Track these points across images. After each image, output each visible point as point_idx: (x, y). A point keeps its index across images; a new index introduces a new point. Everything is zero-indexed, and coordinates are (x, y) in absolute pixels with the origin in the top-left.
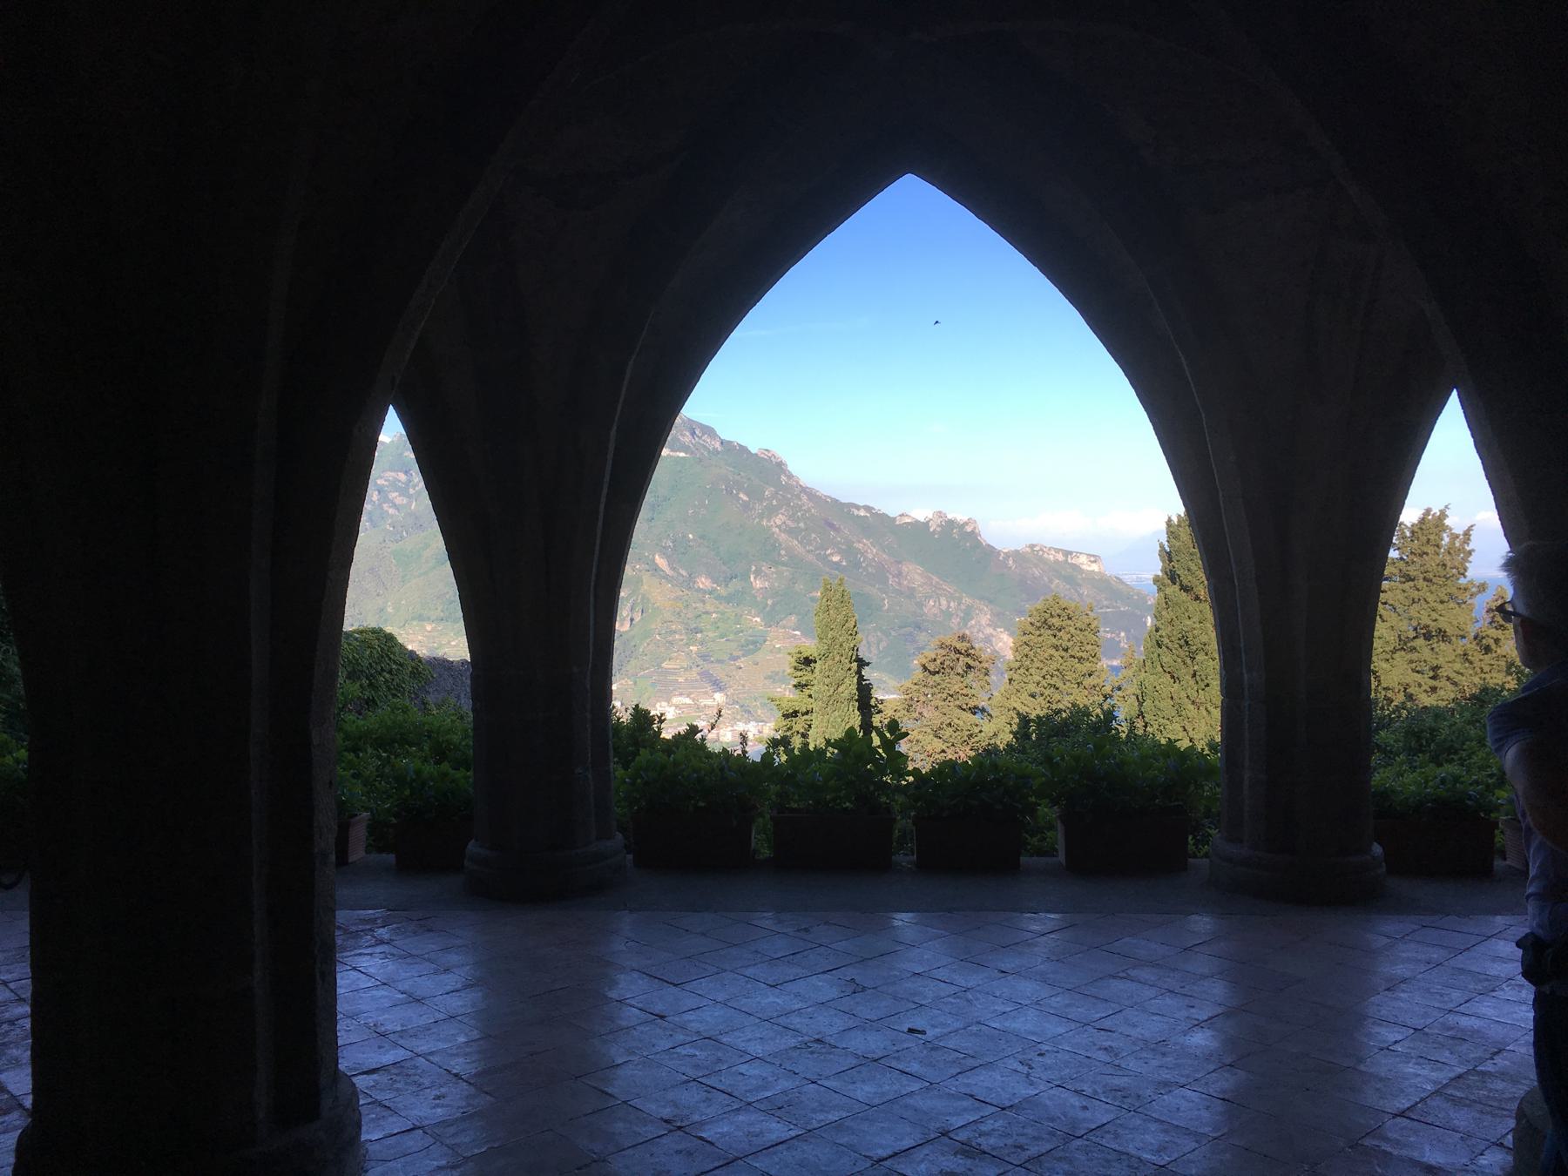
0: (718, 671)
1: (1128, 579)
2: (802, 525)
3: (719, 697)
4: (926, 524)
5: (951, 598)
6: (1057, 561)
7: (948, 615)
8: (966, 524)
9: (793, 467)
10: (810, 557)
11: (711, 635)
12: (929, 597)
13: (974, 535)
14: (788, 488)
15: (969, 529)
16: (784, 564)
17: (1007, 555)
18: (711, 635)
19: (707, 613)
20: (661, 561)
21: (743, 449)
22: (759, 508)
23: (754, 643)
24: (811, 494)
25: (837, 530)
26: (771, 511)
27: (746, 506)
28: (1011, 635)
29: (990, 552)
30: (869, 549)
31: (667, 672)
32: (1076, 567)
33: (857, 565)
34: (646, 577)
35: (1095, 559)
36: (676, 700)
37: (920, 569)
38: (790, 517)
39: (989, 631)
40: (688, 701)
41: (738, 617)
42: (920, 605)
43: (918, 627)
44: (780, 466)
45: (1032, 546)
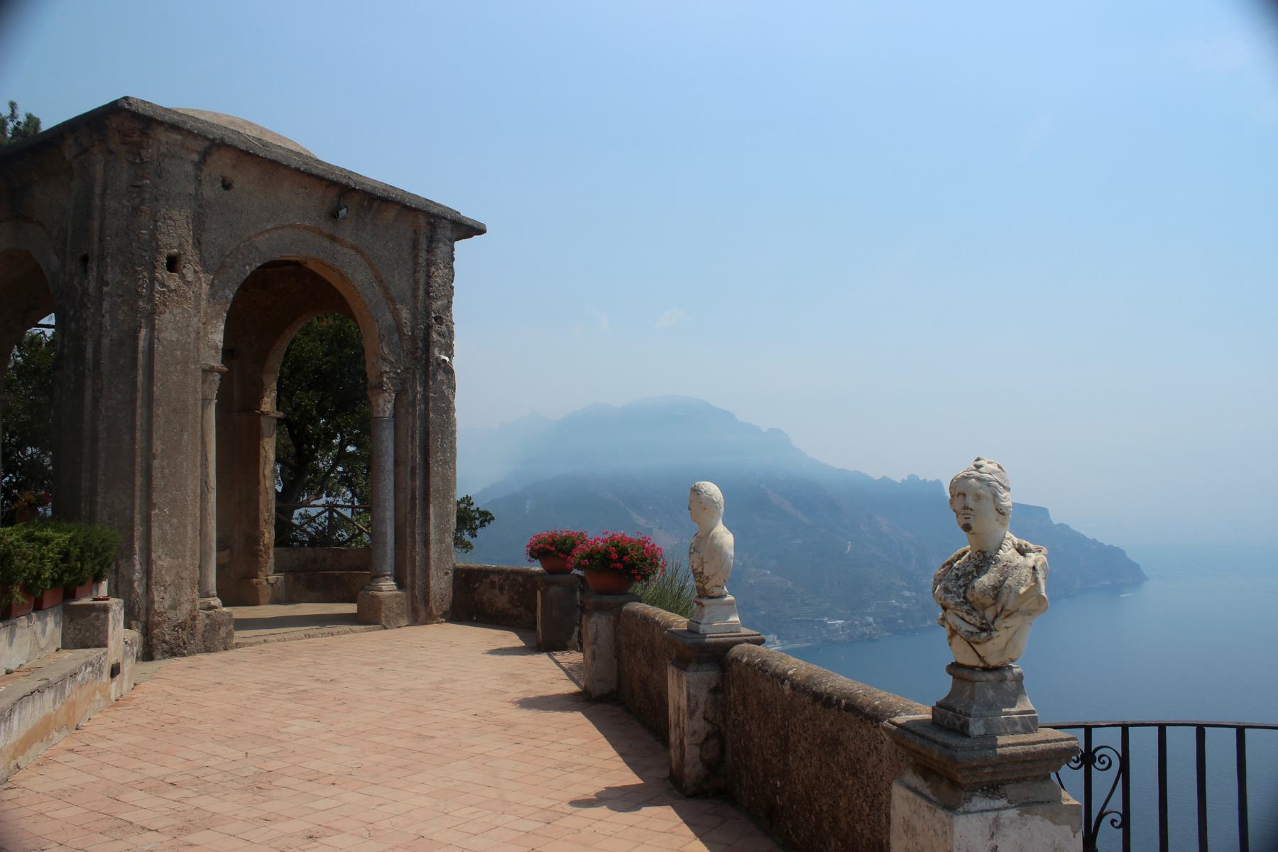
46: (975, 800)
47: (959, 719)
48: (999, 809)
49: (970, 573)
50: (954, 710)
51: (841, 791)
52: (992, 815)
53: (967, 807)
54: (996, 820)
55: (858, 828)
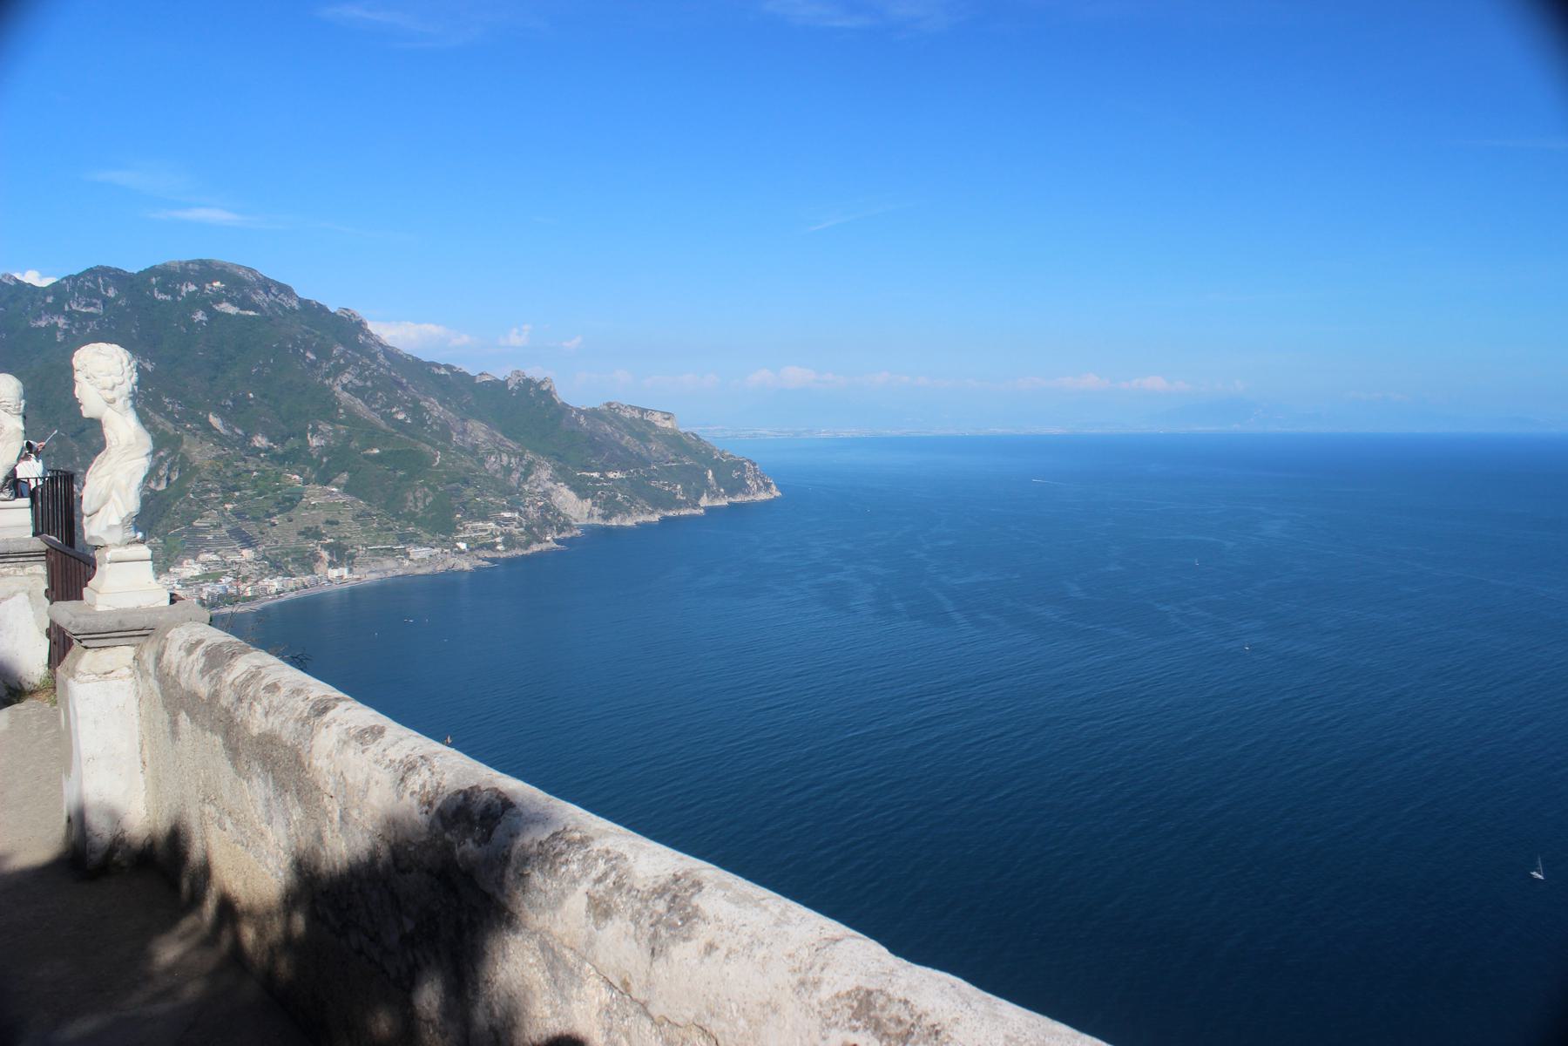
0: (251, 528)
1: (705, 437)
2: (369, 384)
3: (248, 554)
4: (505, 383)
5: (512, 453)
6: (632, 419)
7: (508, 470)
9: (372, 327)
10: (375, 417)
11: (249, 492)
13: (548, 393)
14: (364, 349)
15: (545, 388)
16: (341, 422)
17: (580, 412)
18: (249, 492)
19: (249, 472)
20: (215, 421)
21: (322, 309)
22: (326, 366)
23: (291, 500)
24: (390, 353)
25: (404, 389)
26: (338, 370)
27: (313, 364)
29: (564, 409)
30: (435, 409)
31: (197, 530)
32: (650, 424)
33: (423, 423)
34: (185, 438)
35: (669, 416)
36: (202, 557)
37: (484, 427)
38: (358, 376)
39: (550, 485)
40: (215, 557)
41: (278, 475)
42: (482, 461)
43: (466, 482)
44: (360, 326)
45: (609, 404)
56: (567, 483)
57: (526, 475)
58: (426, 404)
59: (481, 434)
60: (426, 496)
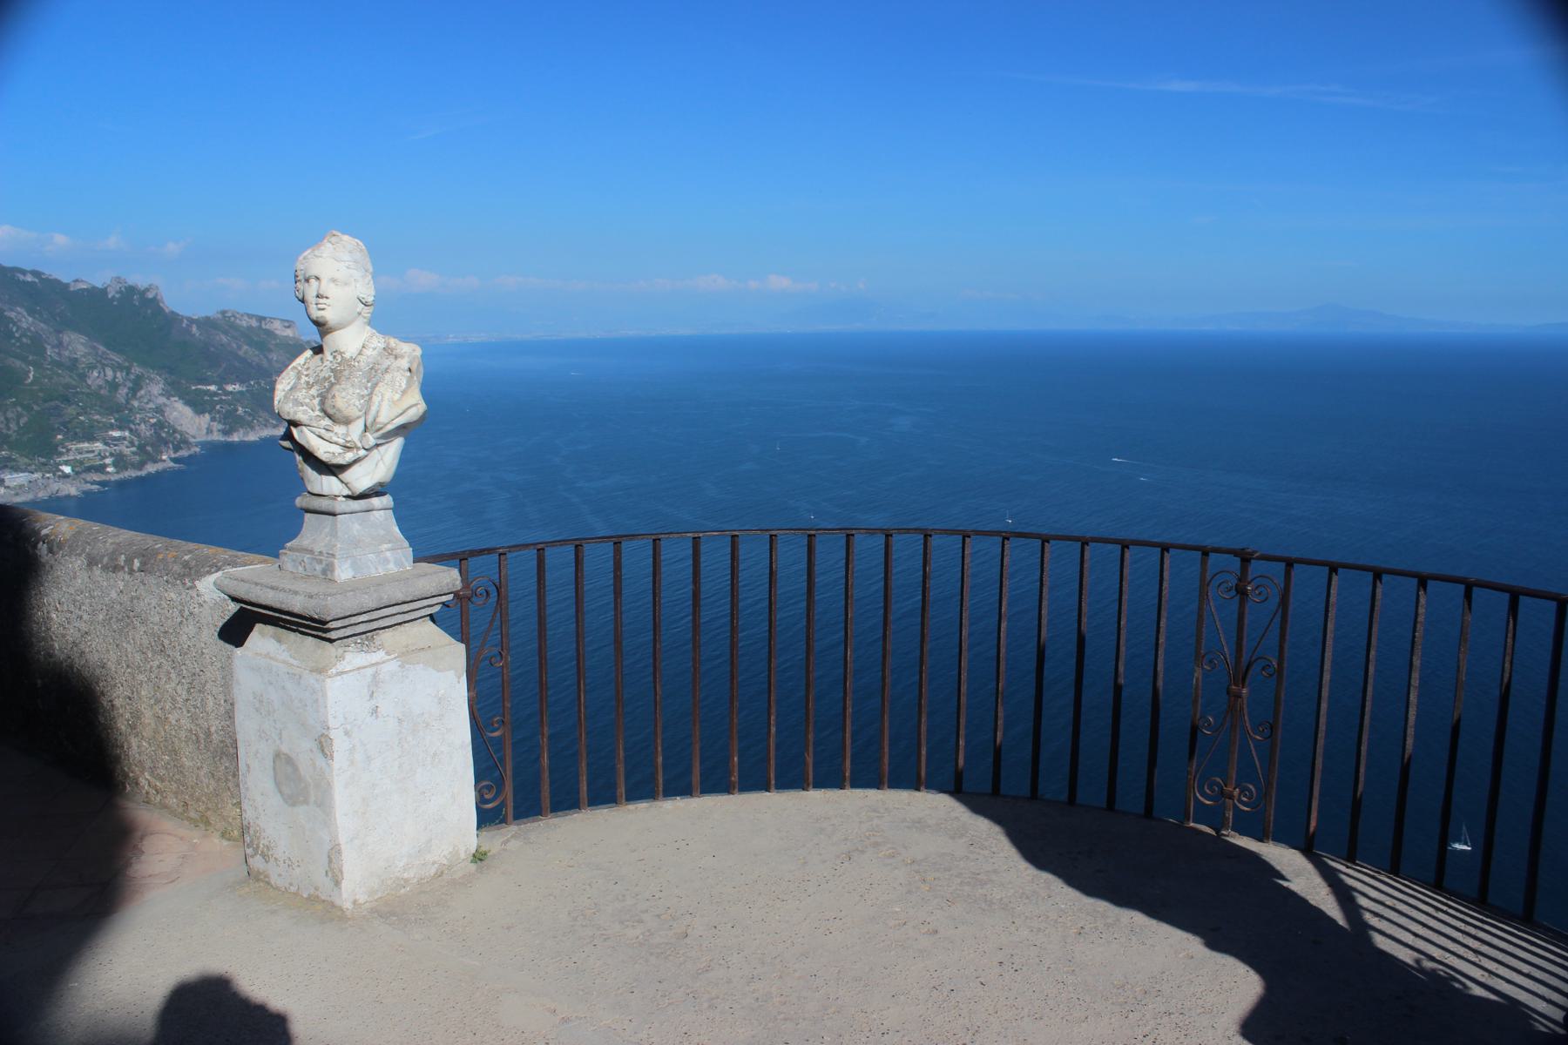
4: (104, 291)
5: (117, 367)
6: (250, 328)
7: (114, 386)
8: (147, 290)
12: (92, 367)
13: (155, 302)
15: (150, 295)
17: (191, 321)
28: (188, 403)
29: (174, 318)
30: (24, 320)
32: (270, 333)
37: (83, 339)
39: (162, 400)
42: (83, 377)
43: (66, 400)
45: (224, 312)
46: (348, 656)
47: (320, 562)
48: (377, 664)
49: (325, 379)
50: (311, 552)
51: (141, 677)
52: (370, 671)
53: (341, 667)
54: (375, 676)
55: (172, 718)
56: (181, 398)
57: (135, 390)
58: (13, 315)
59: (81, 347)
60: (19, 416)
